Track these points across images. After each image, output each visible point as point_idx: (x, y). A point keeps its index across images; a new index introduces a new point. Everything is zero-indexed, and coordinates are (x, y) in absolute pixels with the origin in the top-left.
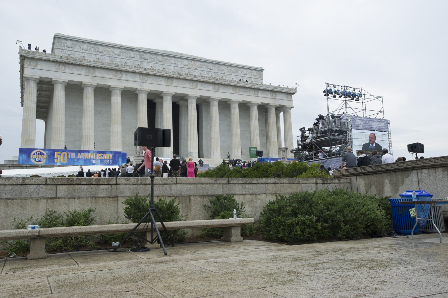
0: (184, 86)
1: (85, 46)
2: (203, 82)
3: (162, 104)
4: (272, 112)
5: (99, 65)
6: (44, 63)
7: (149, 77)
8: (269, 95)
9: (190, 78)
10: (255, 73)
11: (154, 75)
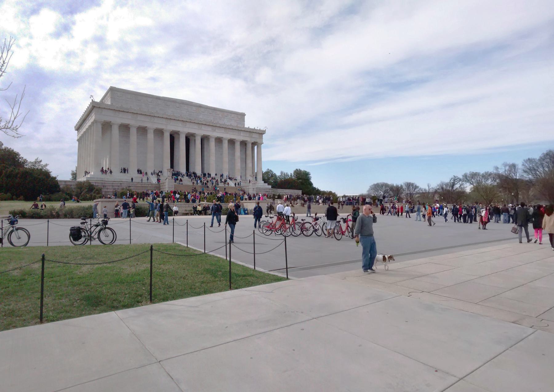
3: (179, 138)
4: (249, 146)
5: (140, 113)
7: (172, 121)
8: (248, 134)
10: (239, 117)
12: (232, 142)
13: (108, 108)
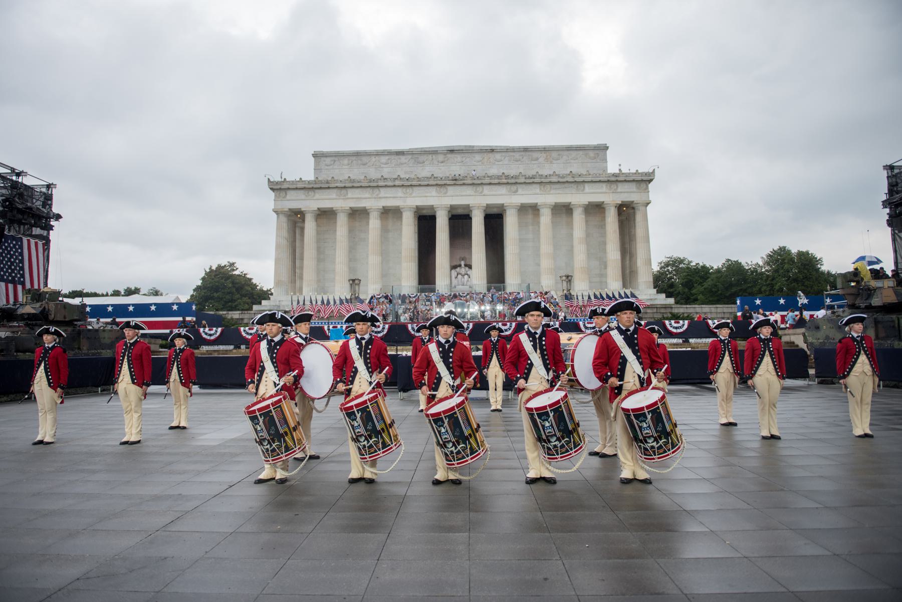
0: (464, 193)
1: (346, 161)
2: (490, 184)
5: (350, 185)
6: (292, 192)
7: (415, 188)
8: (604, 187)
9: (470, 182)
10: (592, 154)
11: (420, 185)
12: (564, 210)
13: (294, 186)
